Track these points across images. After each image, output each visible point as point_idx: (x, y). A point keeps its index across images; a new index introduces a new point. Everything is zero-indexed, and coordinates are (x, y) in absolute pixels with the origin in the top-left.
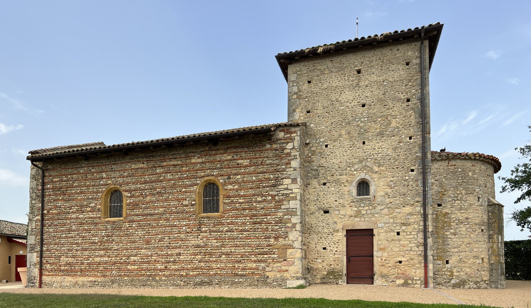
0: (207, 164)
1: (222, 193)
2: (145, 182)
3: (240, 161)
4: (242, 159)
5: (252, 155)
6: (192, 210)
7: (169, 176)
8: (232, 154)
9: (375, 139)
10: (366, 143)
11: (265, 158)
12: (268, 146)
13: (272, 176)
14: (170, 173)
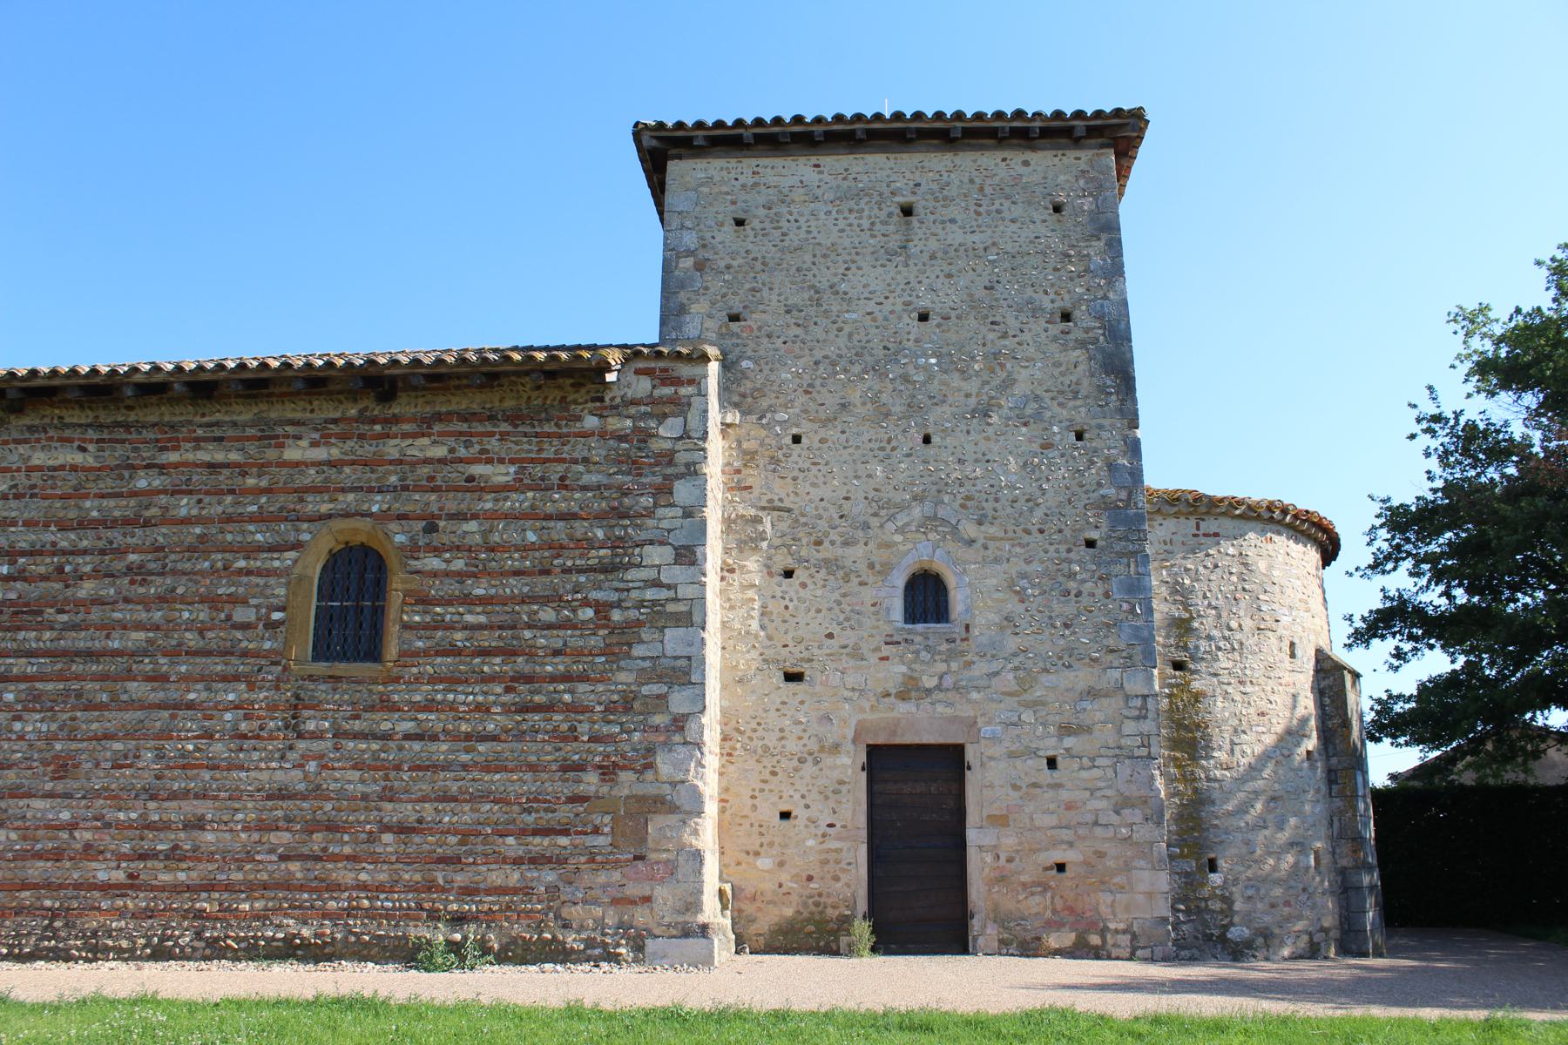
0: (347, 470)
1: (398, 586)
2: (83, 524)
3: (478, 470)
4: (489, 461)
5: (528, 448)
6: (267, 645)
7: (184, 506)
8: (451, 442)
9: (965, 428)
10: (935, 439)
11: (575, 462)
12: (591, 422)
13: (600, 534)
14: (190, 492)
